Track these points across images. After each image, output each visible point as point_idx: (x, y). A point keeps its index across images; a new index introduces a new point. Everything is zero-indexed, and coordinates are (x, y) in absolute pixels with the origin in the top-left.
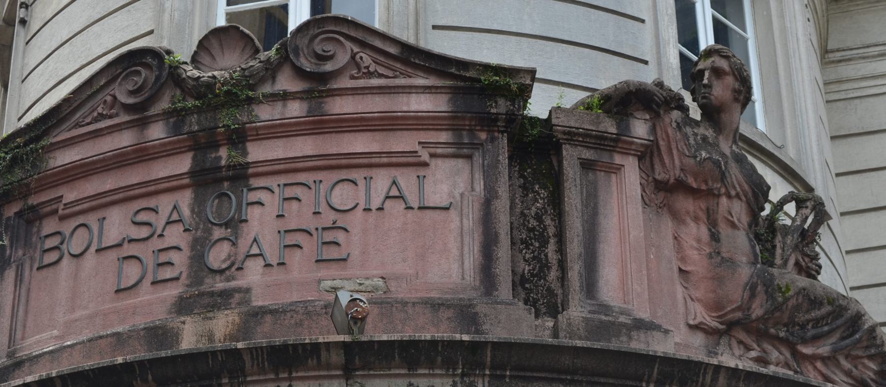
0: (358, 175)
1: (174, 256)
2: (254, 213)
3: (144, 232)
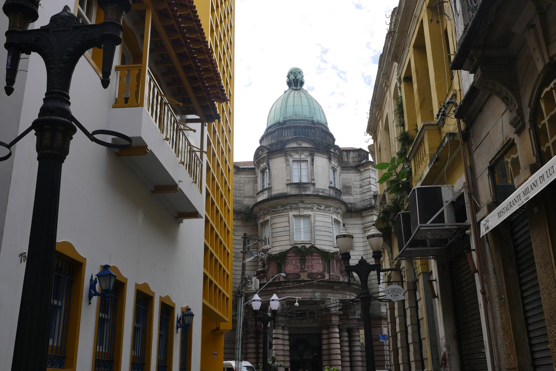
0: (314, 260)
1: (299, 266)
3: (296, 263)
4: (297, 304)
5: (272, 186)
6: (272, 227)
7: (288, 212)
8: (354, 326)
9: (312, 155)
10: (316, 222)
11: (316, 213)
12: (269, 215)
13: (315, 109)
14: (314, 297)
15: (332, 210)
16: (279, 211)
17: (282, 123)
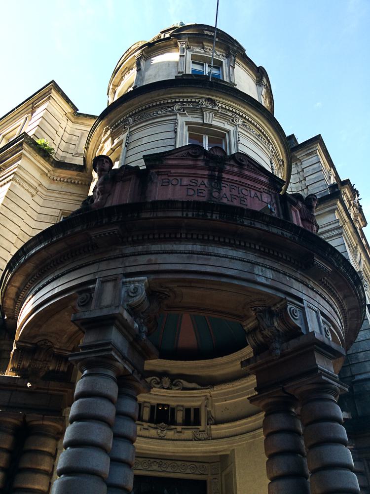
3: (194, 184)
7: (176, 115)
11: (239, 130)
14: (249, 276)
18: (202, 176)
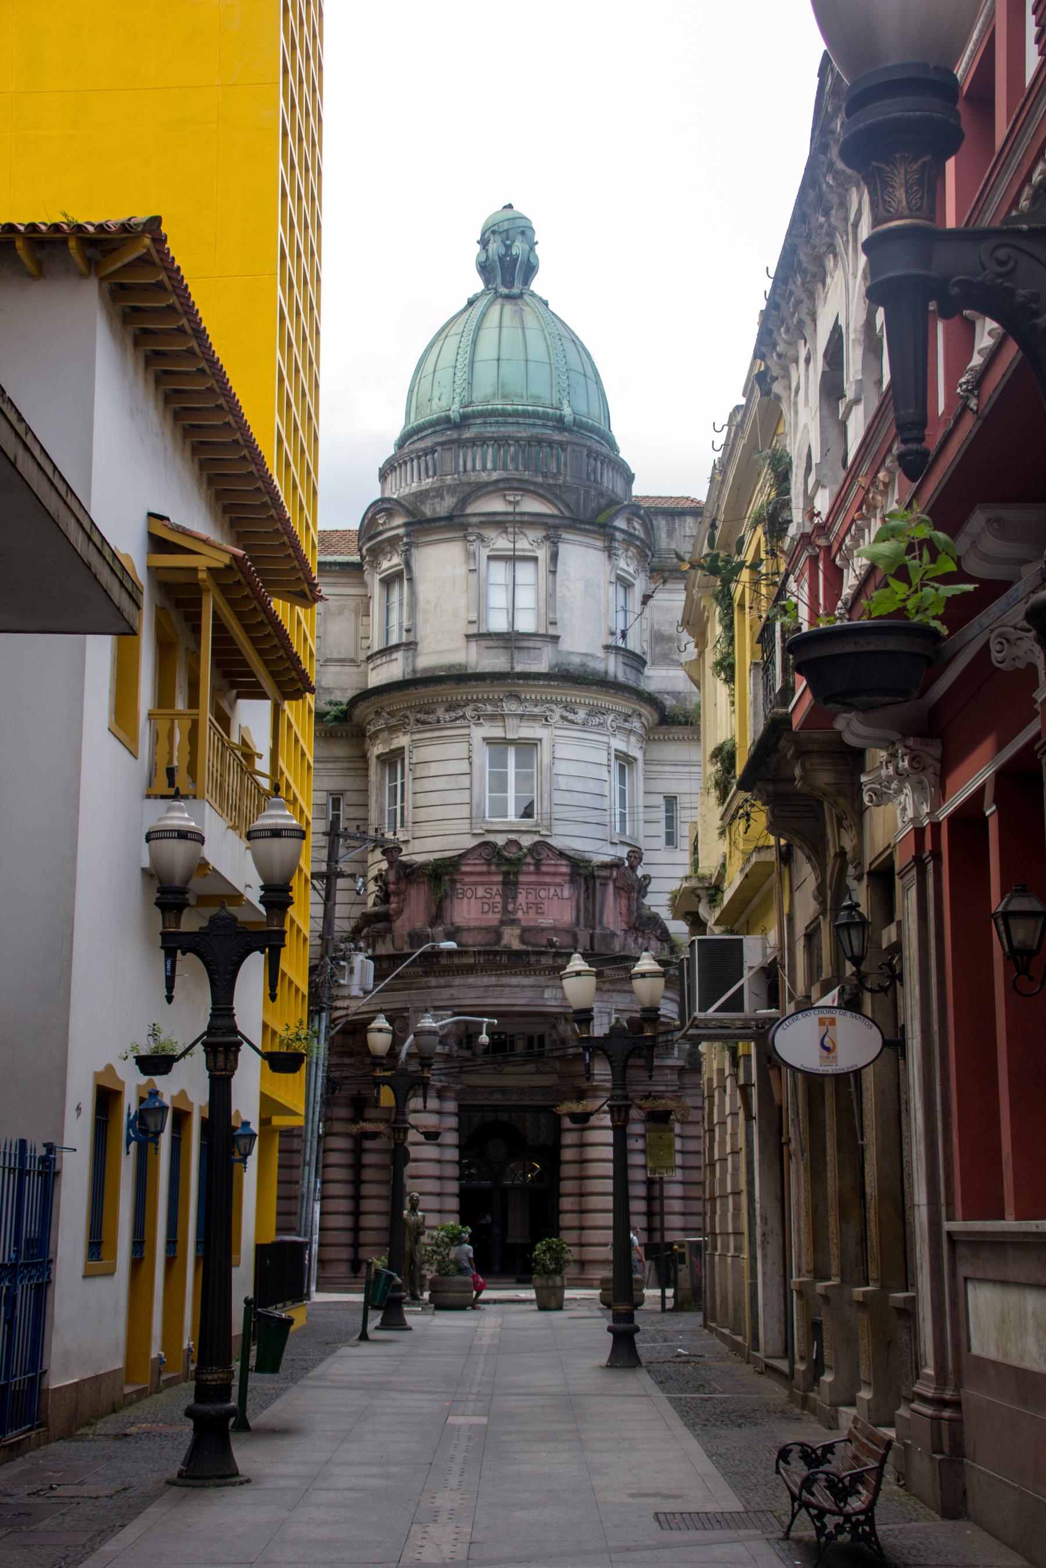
2: (520, 896)
4: (484, 1038)
5: (418, 639)
6: (414, 773)
8: (663, 1088)
9: (553, 540)
10: (556, 761)
12: (405, 733)
13: (572, 375)
14: (539, 1002)
15: (609, 723)
16: (439, 721)
17: (458, 420)
18: (496, 883)
